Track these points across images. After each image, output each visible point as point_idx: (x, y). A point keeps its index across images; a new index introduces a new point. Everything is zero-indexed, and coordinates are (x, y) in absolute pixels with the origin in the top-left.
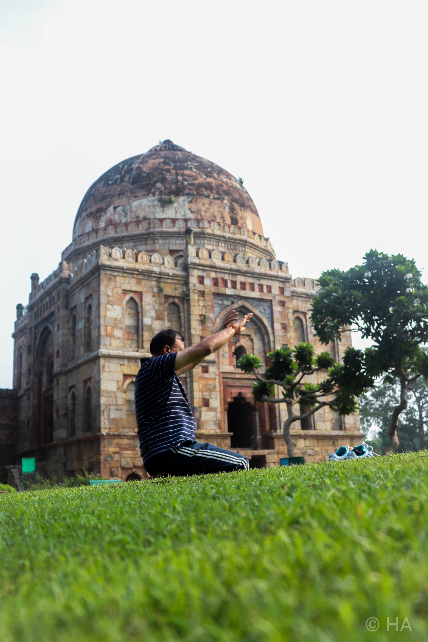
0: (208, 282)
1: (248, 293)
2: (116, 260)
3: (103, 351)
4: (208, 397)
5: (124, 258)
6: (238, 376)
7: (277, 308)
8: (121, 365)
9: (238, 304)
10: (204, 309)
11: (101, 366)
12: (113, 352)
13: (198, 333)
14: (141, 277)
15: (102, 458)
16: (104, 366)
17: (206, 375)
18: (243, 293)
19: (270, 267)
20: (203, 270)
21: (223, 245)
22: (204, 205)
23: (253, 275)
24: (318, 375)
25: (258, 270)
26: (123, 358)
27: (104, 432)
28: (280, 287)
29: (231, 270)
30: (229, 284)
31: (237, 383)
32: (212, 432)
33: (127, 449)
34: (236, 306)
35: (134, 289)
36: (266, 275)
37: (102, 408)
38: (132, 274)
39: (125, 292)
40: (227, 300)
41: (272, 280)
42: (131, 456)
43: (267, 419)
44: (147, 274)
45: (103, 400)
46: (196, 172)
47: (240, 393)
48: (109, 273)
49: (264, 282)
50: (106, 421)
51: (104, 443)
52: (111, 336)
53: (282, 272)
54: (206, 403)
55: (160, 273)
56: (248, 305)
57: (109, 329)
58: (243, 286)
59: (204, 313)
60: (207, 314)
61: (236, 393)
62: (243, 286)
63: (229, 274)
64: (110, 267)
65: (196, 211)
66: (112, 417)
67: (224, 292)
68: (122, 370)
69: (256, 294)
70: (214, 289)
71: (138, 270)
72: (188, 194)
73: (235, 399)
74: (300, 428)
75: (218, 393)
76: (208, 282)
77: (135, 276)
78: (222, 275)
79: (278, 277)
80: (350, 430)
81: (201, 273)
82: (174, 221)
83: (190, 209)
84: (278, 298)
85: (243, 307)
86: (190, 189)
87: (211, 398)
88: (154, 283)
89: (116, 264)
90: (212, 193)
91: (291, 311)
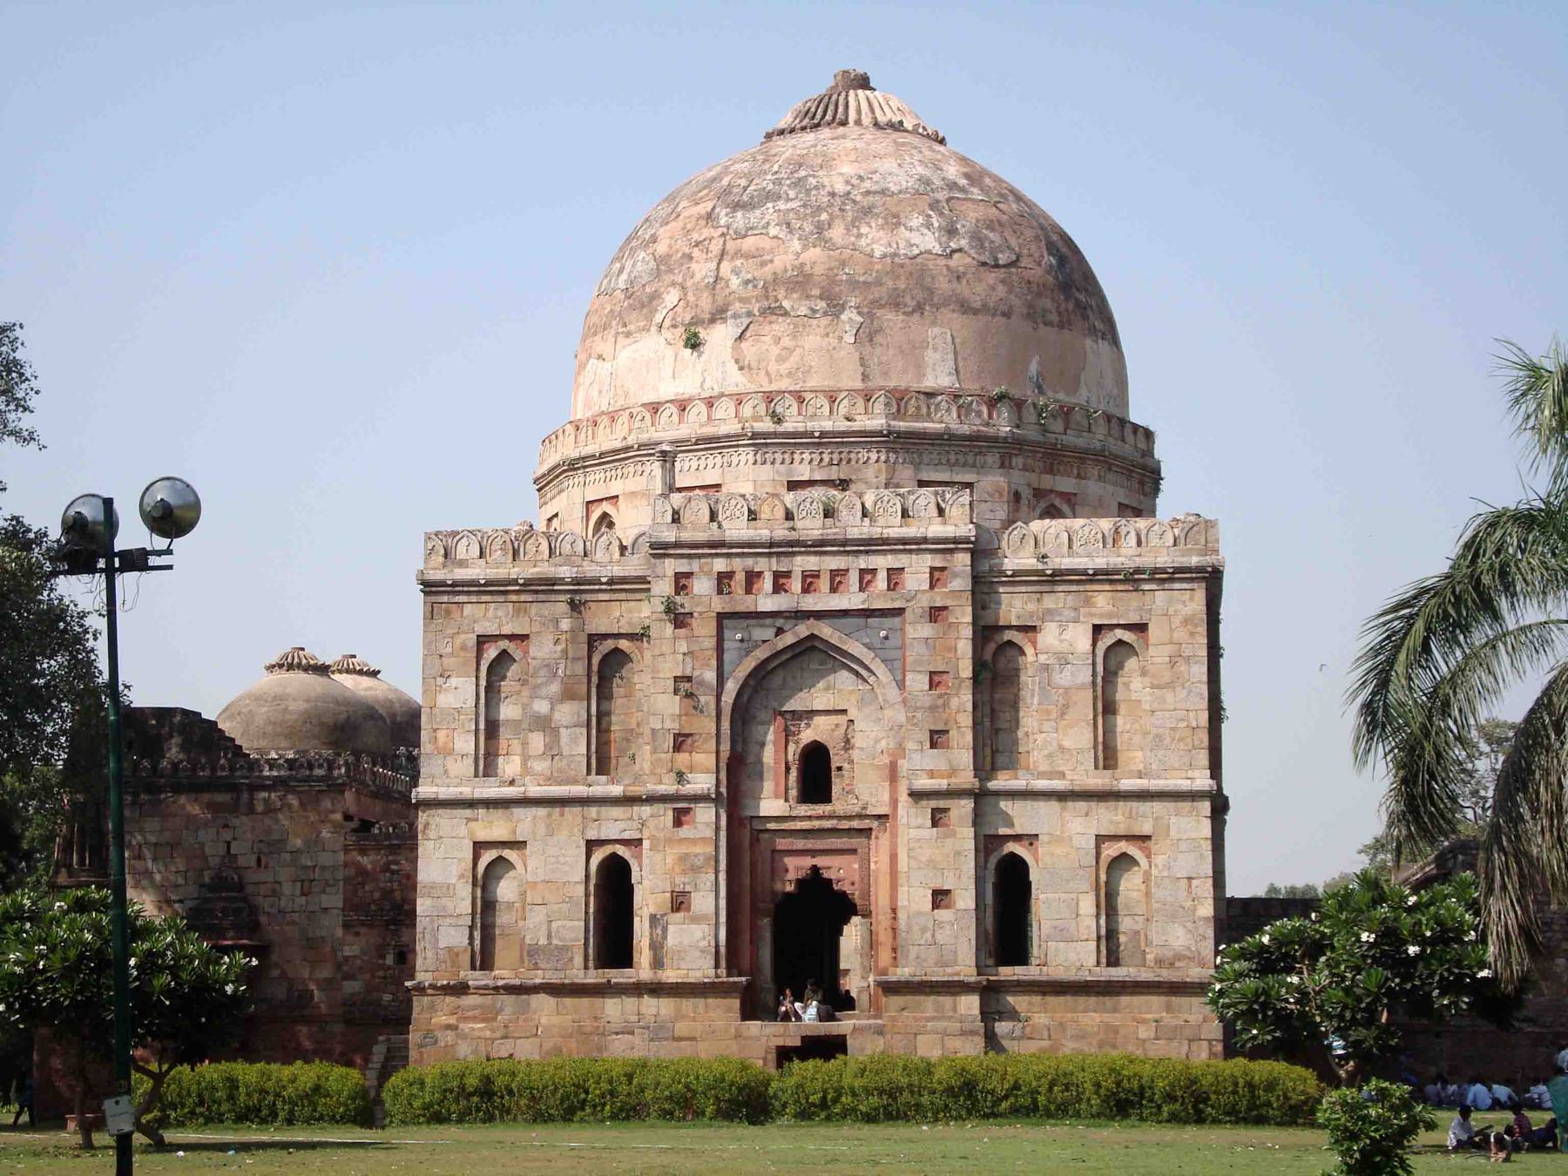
0: (702, 586)
1: (822, 600)
2: (462, 564)
3: (424, 790)
4: (688, 888)
5: (482, 555)
6: (799, 825)
7: (918, 631)
8: (469, 820)
9: (796, 634)
10: (688, 659)
11: (420, 827)
12: (445, 792)
13: (668, 725)
14: (529, 598)
15: (414, 1037)
16: (427, 825)
17: (685, 832)
18: (811, 603)
19: (905, 514)
20: (689, 556)
21: (806, 456)
22: (777, 340)
23: (845, 546)
24: (1064, 809)
25: (858, 529)
26: (471, 804)
27: (423, 977)
28: (933, 569)
29: (771, 545)
30: (767, 583)
31: (800, 844)
32: (695, 977)
33: (474, 1019)
34: (789, 639)
35: (506, 630)
36: (885, 541)
37: (421, 922)
38: (506, 592)
39: (482, 641)
40: (762, 626)
41: (910, 551)
42: (482, 1034)
43: (884, 937)
44: (542, 587)
45: (423, 906)
46: (775, 237)
47: (815, 869)
48: (445, 598)
49: (882, 562)
50: (430, 954)
51: (419, 1003)
52: (448, 752)
53: (945, 523)
54: (679, 902)
55: (577, 581)
56: (825, 630)
57: (441, 735)
58: (809, 582)
59: (688, 673)
60: (696, 673)
61: (798, 869)
62: (809, 582)
63: (770, 555)
64: (443, 584)
65: (753, 364)
66: (441, 945)
67: (752, 609)
68: (471, 833)
69: (851, 599)
70: (719, 604)
71: (515, 582)
72: (735, 316)
73: (800, 882)
74: (990, 962)
75: (722, 877)
76: (702, 586)
77: (514, 598)
78: (750, 562)
79: (925, 540)
80: (1172, 964)
81: (682, 565)
82: (683, 406)
83: (737, 361)
84: (925, 601)
85: (812, 637)
86: (741, 300)
87: (696, 889)
88: (564, 607)
89: (461, 574)
90: (808, 297)
91: (967, 632)
